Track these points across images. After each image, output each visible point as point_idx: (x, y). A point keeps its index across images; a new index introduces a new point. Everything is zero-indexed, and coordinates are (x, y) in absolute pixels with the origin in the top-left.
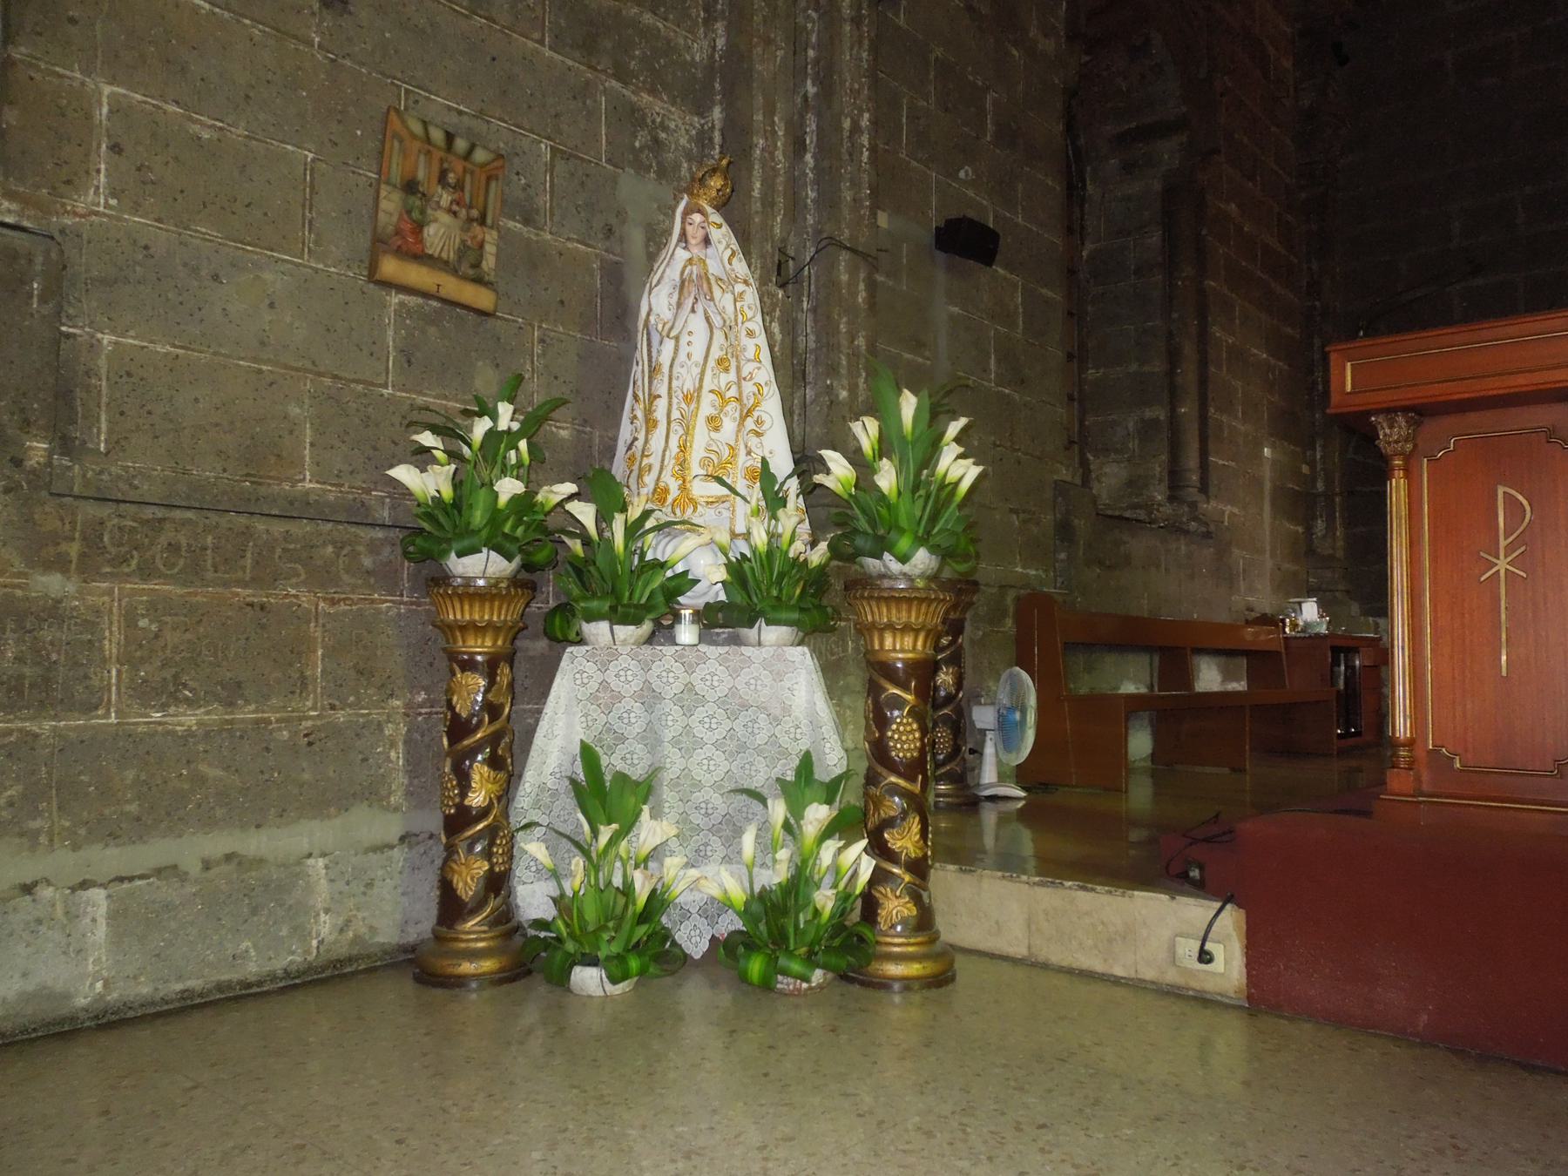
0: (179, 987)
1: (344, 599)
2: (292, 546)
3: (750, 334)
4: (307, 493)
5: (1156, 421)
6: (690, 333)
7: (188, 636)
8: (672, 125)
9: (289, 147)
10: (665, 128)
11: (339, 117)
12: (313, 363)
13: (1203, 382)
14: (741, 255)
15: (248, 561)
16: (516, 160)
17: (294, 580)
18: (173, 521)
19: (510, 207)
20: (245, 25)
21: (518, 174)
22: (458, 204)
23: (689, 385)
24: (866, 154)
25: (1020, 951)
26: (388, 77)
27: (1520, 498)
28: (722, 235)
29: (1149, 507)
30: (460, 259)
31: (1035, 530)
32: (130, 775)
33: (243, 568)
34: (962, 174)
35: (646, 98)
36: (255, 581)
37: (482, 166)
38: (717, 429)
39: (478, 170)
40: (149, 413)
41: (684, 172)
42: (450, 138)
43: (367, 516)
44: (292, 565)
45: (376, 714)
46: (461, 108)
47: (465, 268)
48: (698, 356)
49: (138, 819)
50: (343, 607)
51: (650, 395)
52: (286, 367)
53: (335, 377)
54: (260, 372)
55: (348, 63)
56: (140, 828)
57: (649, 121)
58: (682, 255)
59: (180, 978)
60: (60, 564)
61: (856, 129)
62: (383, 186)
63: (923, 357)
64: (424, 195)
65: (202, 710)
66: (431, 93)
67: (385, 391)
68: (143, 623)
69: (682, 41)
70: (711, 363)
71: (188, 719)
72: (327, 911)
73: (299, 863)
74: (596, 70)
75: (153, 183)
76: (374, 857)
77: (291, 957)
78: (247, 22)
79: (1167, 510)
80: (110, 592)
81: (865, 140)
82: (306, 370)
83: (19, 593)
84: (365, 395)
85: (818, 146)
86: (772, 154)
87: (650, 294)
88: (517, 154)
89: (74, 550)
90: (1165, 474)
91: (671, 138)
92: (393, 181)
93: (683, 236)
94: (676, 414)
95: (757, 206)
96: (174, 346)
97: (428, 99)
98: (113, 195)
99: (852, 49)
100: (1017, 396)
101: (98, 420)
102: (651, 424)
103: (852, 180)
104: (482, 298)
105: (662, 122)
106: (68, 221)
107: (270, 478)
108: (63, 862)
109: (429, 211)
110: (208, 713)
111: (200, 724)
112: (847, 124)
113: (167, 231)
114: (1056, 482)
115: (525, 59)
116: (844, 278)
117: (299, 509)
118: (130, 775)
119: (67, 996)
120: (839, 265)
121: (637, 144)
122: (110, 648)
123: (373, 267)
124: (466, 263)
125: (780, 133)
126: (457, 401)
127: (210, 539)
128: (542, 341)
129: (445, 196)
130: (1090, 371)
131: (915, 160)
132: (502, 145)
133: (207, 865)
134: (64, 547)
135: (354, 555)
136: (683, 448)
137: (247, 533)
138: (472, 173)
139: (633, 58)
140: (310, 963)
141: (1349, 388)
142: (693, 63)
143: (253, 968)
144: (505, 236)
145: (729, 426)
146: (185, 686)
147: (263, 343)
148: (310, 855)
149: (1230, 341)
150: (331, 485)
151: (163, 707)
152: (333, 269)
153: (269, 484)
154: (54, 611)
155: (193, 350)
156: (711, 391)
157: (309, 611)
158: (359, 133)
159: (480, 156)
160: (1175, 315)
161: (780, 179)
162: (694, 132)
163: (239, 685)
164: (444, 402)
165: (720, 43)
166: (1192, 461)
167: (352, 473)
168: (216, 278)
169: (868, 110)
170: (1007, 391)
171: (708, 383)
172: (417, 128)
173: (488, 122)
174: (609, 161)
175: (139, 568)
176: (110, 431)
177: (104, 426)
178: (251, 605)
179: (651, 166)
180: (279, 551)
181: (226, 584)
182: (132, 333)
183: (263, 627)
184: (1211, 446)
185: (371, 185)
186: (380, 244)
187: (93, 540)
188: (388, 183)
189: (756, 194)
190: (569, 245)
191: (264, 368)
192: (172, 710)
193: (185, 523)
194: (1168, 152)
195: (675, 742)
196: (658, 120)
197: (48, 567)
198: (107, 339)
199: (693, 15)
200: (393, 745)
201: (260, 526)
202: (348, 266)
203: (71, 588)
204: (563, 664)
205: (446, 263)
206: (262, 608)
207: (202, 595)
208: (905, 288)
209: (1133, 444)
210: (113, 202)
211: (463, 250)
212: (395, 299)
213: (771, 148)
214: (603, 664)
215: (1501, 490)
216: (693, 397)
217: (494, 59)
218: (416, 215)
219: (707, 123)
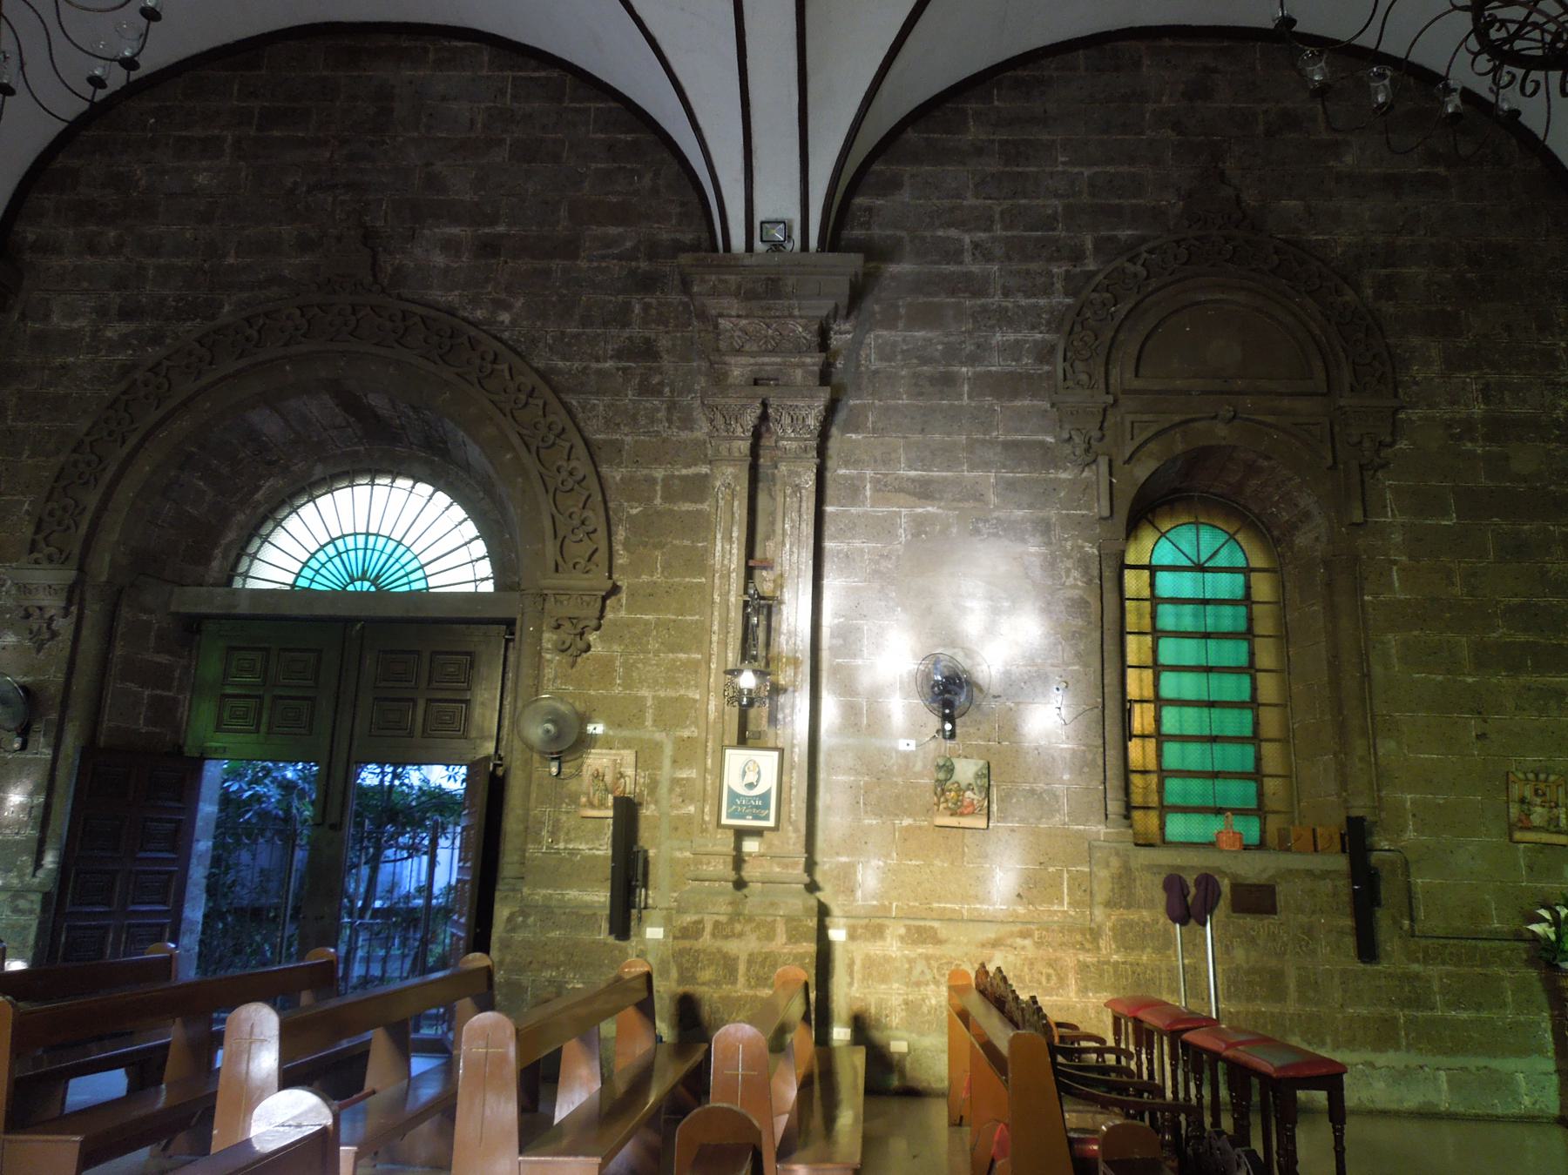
30: (1549, 824)
42: (1537, 775)
47: (1552, 828)
50: (1516, 975)
53: (1501, 882)
60: (1417, 960)
68: (1445, 980)
71: (1464, 1015)
73: (1513, 1074)
76: (1543, 1077)
77: (1515, 1111)
89: (1420, 955)
108: (1431, 1060)
117: (1494, 936)
118: (1447, 1033)
119: (1437, 1105)
122: (1436, 988)
123: (1511, 839)
124: (1553, 826)
133: (1478, 1069)
143: (1500, 1111)
147: (1472, 873)
154: (1417, 976)
159: (1552, 778)
172: (1521, 776)
186: (1511, 828)
187: (1426, 951)
193: (1455, 945)
197: (1413, 962)
198: (1419, 881)
200: (1546, 1032)
201: (1481, 944)
205: (1543, 827)
206: (1486, 975)
207: (1463, 970)
211: (1550, 821)
212: (1522, 846)
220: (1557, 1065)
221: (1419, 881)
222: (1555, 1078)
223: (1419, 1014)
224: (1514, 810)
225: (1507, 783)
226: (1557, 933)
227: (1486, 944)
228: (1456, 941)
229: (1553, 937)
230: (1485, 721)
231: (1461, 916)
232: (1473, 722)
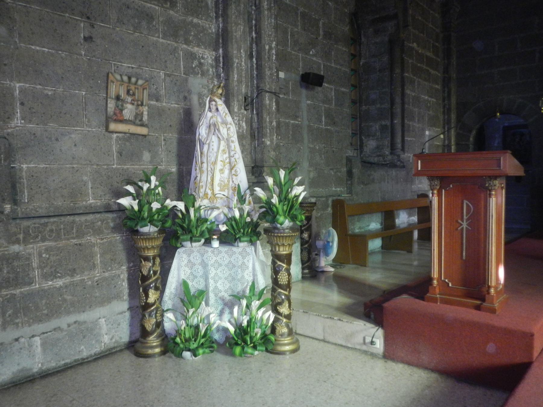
0: (63, 362)
1: (105, 238)
2: (88, 224)
3: (233, 142)
4: (91, 204)
5: (386, 125)
6: (213, 142)
7: (58, 257)
8: (206, 57)
9: (77, 92)
10: (203, 58)
11: (92, 78)
12: (90, 162)
13: (403, 110)
14: (229, 114)
15: (74, 231)
16: (152, 80)
17: (89, 234)
18: (50, 222)
19: (151, 97)
20: (60, 54)
21: (153, 85)
22: (134, 101)
23: (213, 159)
24: (274, 57)
25: (321, 337)
26: (107, 60)
27: (470, 205)
28: (222, 107)
29: (383, 156)
31: (339, 174)
32: (44, 302)
33: (73, 233)
34: (311, 53)
35: (196, 49)
36: (78, 237)
37: (141, 86)
38: (223, 173)
39: (139, 87)
40: (40, 187)
41: (211, 72)
42: (130, 78)
43: (110, 208)
44: (88, 230)
45: (118, 272)
46: (133, 66)
47: (137, 122)
48: (215, 150)
49: (47, 315)
50: (105, 240)
51: (201, 161)
52: (81, 164)
53: (98, 165)
54: (73, 167)
55: (94, 59)
56: (49, 317)
57: (197, 57)
58: (209, 114)
59: (63, 360)
60: (17, 242)
61: (271, 48)
62: (108, 99)
63: (298, 121)
64: (122, 100)
65: (64, 279)
66: (122, 63)
67: (114, 167)
68: (44, 255)
69: (207, 26)
70: (220, 151)
71: (59, 283)
72: (106, 334)
73: (97, 321)
74: (178, 42)
75: (35, 112)
76: (120, 316)
78: (60, 52)
79: (390, 157)
80: (33, 248)
81: (274, 52)
82: (88, 164)
83: (6, 252)
84: (107, 169)
85: (257, 56)
86: (241, 64)
87: (199, 129)
88: (153, 78)
89: (21, 236)
90: (389, 145)
91: (205, 61)
92: (112, 97)
93: (210, 108)
94: (209, 169)
95: (235, 83)
96: (45, 164)
97: (121, 65)
98: (23, 119)
99: (268, 20)
100: (332, 129)
101: (24, 192)
102: (202, 172)
103: (269, 67)
104: (143, 131)
105: (202, 57)
106: (9, 131)
107: (80, 201)
108: (27, 330)
109: (124, 105)
110: (66, 280)
111: (64, 283)
112: (267, 47)
113: (40, 127)
114: (347, 157)
115: (153, 44)
116: (268, 102)
118: (44, 302)
119: (31, 369)
120: (266, 97)
121: (194, 66)
122: (35, 265)
124: (137, 120)
125: (243, 56)
126: (137, 165)
127: (62, 226)
128: (165, 140)
129: (129, 98)
130: (363, 107)
131: (294, 51)
132: (147, 76)
133: (69, 326)
134: (18, 236)
135: (107, 223)
136: (212, 180)
137: (74, 222)
138: (138, 89)
139: (191, 35)
140: (102, 350)
141: (419, 169)
142: (212, 33)
143: (85, 354)
144: (149, 106)
145: (227, 172)
146: (58, 272)
147: (73, 158)
148: (100, 318)
149: (413, 95)
150: (99, 200)
151: (52, 280)
152: (94, 130)
153: (79, 203)
154: (17, 256)
155: (52, 165)
156: (221, 161)
157: (94, 243)
158: (99, 82)
159: (140, 82)
160: (393, 87)
161: (243, 73)
162: (213, 57)
163: (74, 269)
164: (133, 167)
165: (221, 25)
166: (399, 140)
167: (105, 195)
168: (57, 140)
169: (275, 41)
170: (329, 128)
171: (219, 158)
172: (118, 77)
173: (142, 69)
174: (184, 74)
175: (41, 239)
176: (28, 195)
177: (26, 194)
178: (76, 244)
179: (199, 73)
180: (84, 226)
181: (68, 239)
182: (32, 163)
183: (81, 251)
184: (406, 133)
185: (104, 99)
187: (27, 233)
188: (110, 98)
189: (235, 79)
190: (172, 105)
191: (74, 166)
192: (55, 280)
193: (54, 222)
194: (390, 26)
195: (212, 278)
196: (201, 56)
197: (14, 243)
198: (24, 166)
199: (212, 16)
200: (123, 281)
201: (77, 219)
202: (99, 128)
203: (21, 248)
204: (176, 255)
205: (131, 121)
206: (80, 244)
208: (291, 98)
209: (378, 134)
210: (23, 121)
212: (115, 135)
213: (240, 62)
214: (189, 254)
215: (465, 202)
216: (215, 163)
217: (143, 47)
218: (120, 107)
219: (217, 54)
220: (130, 303)
221: (24, 166)
222: (128, 314)
223: (18, 291)
224: (111, 105)
225: (107, 83)
226: (140, 204)
227: (83, 218)
228: (55, 219)
229: (136, 208)
230: (92, 26)
231: (62, 196)
232: (82, 25)
